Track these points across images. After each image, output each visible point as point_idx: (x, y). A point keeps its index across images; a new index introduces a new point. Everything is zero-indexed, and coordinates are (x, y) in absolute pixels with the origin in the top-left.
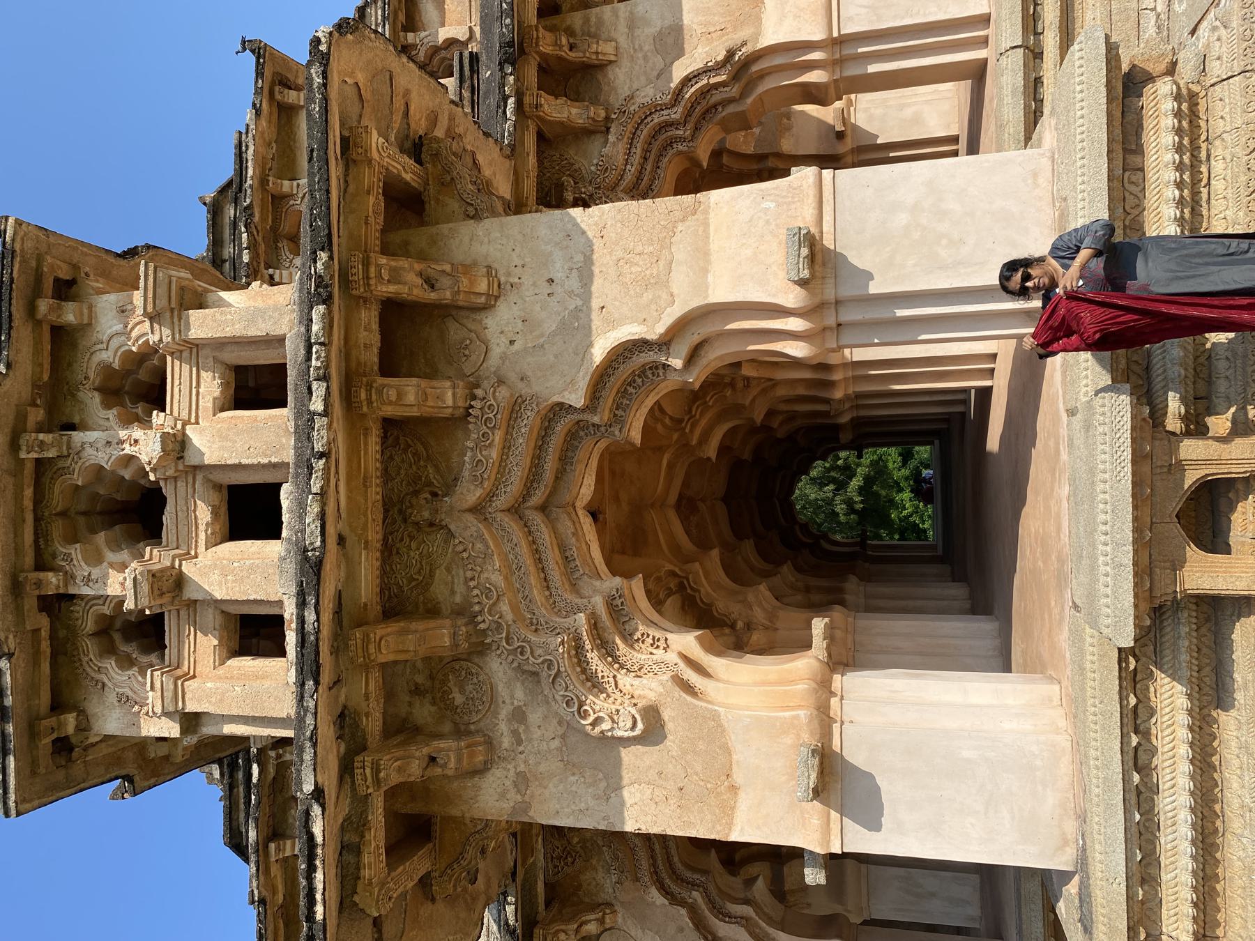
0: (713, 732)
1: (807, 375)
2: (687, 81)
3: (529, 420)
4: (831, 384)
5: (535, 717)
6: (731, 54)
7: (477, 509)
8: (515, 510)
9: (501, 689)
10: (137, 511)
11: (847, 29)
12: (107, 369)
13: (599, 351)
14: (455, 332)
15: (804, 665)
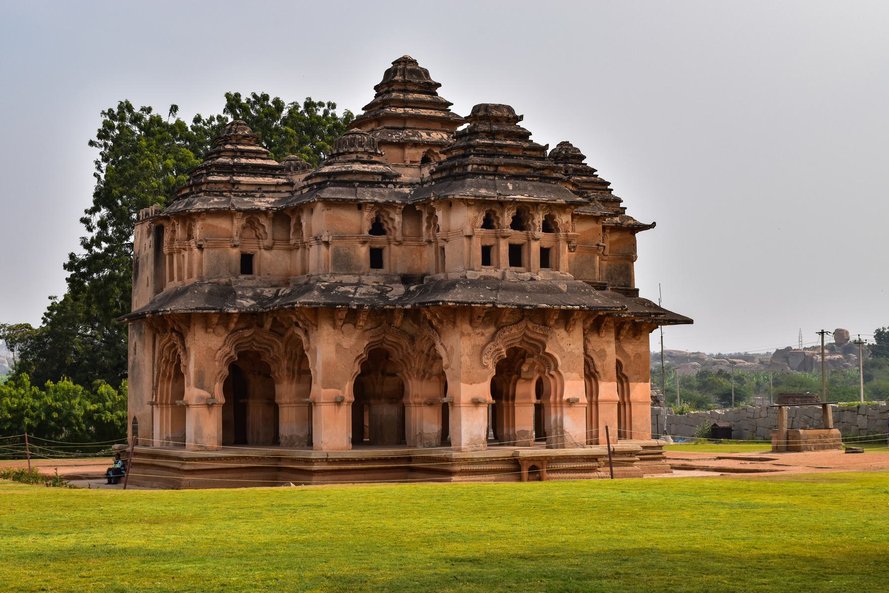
0: (484, 380)
1: (510, 393)
2: (592, 359)
3: (543, 339)
4: (507, 399)
5: (483, 338)
6: (597, 372)
7: (527, 327)
8: (525, 335)
9: (487, 330)
10: (518, 223)
11: (601, 406)
12: (554, 217)
13: (556, 356)
14: (561, 321)
15: (489, 399)
